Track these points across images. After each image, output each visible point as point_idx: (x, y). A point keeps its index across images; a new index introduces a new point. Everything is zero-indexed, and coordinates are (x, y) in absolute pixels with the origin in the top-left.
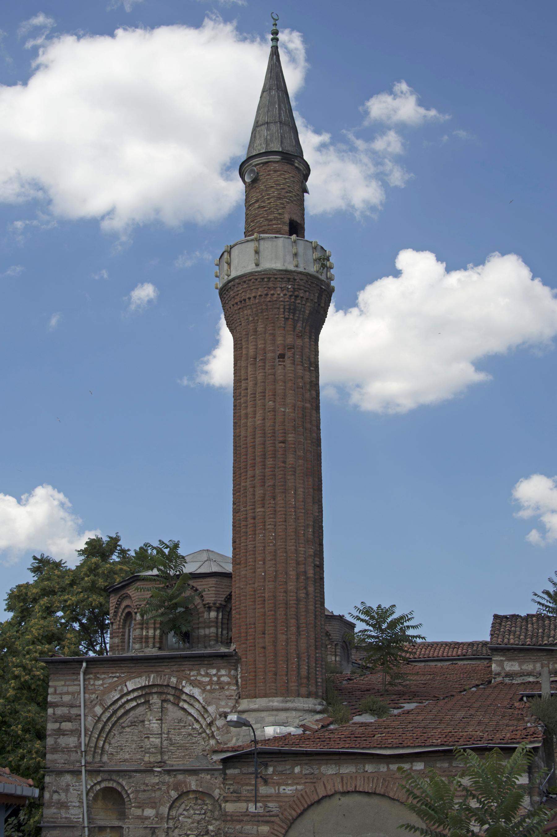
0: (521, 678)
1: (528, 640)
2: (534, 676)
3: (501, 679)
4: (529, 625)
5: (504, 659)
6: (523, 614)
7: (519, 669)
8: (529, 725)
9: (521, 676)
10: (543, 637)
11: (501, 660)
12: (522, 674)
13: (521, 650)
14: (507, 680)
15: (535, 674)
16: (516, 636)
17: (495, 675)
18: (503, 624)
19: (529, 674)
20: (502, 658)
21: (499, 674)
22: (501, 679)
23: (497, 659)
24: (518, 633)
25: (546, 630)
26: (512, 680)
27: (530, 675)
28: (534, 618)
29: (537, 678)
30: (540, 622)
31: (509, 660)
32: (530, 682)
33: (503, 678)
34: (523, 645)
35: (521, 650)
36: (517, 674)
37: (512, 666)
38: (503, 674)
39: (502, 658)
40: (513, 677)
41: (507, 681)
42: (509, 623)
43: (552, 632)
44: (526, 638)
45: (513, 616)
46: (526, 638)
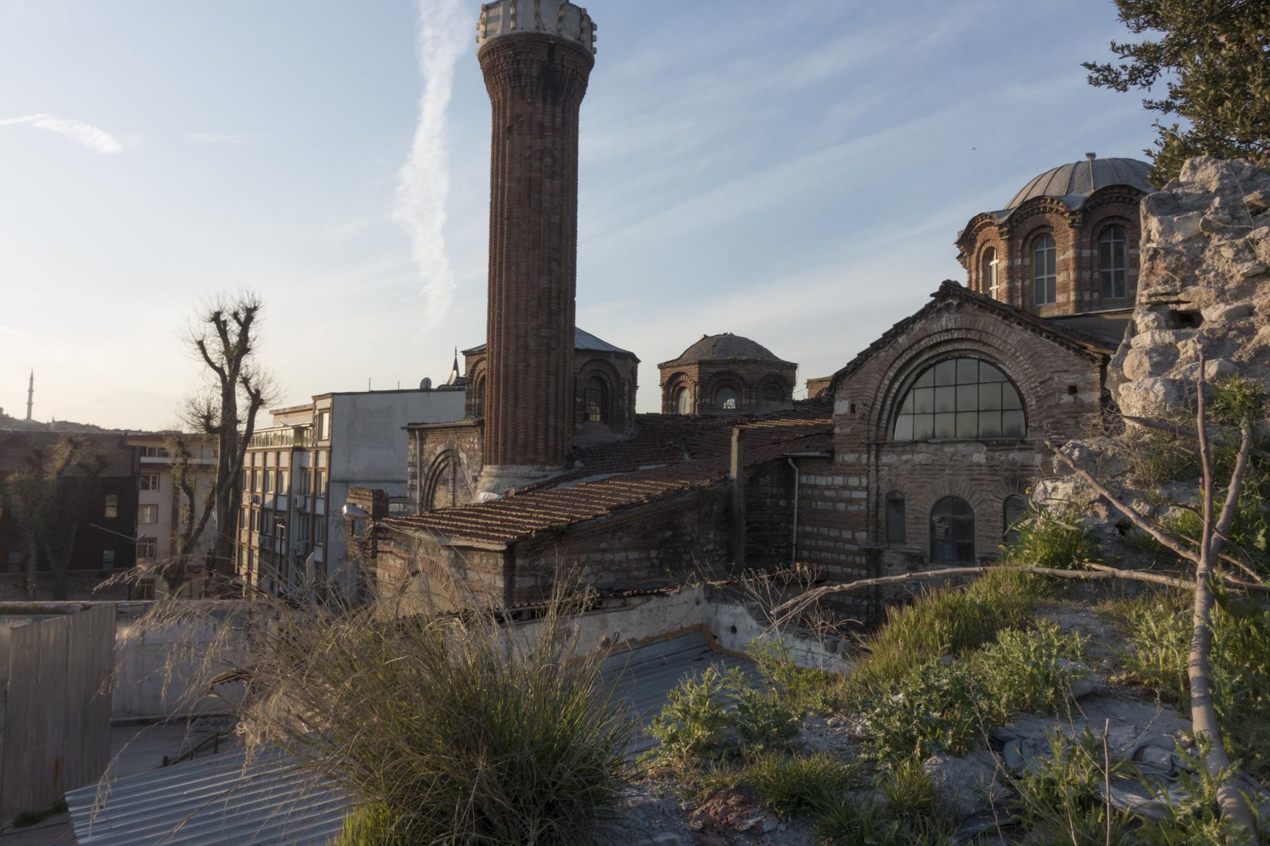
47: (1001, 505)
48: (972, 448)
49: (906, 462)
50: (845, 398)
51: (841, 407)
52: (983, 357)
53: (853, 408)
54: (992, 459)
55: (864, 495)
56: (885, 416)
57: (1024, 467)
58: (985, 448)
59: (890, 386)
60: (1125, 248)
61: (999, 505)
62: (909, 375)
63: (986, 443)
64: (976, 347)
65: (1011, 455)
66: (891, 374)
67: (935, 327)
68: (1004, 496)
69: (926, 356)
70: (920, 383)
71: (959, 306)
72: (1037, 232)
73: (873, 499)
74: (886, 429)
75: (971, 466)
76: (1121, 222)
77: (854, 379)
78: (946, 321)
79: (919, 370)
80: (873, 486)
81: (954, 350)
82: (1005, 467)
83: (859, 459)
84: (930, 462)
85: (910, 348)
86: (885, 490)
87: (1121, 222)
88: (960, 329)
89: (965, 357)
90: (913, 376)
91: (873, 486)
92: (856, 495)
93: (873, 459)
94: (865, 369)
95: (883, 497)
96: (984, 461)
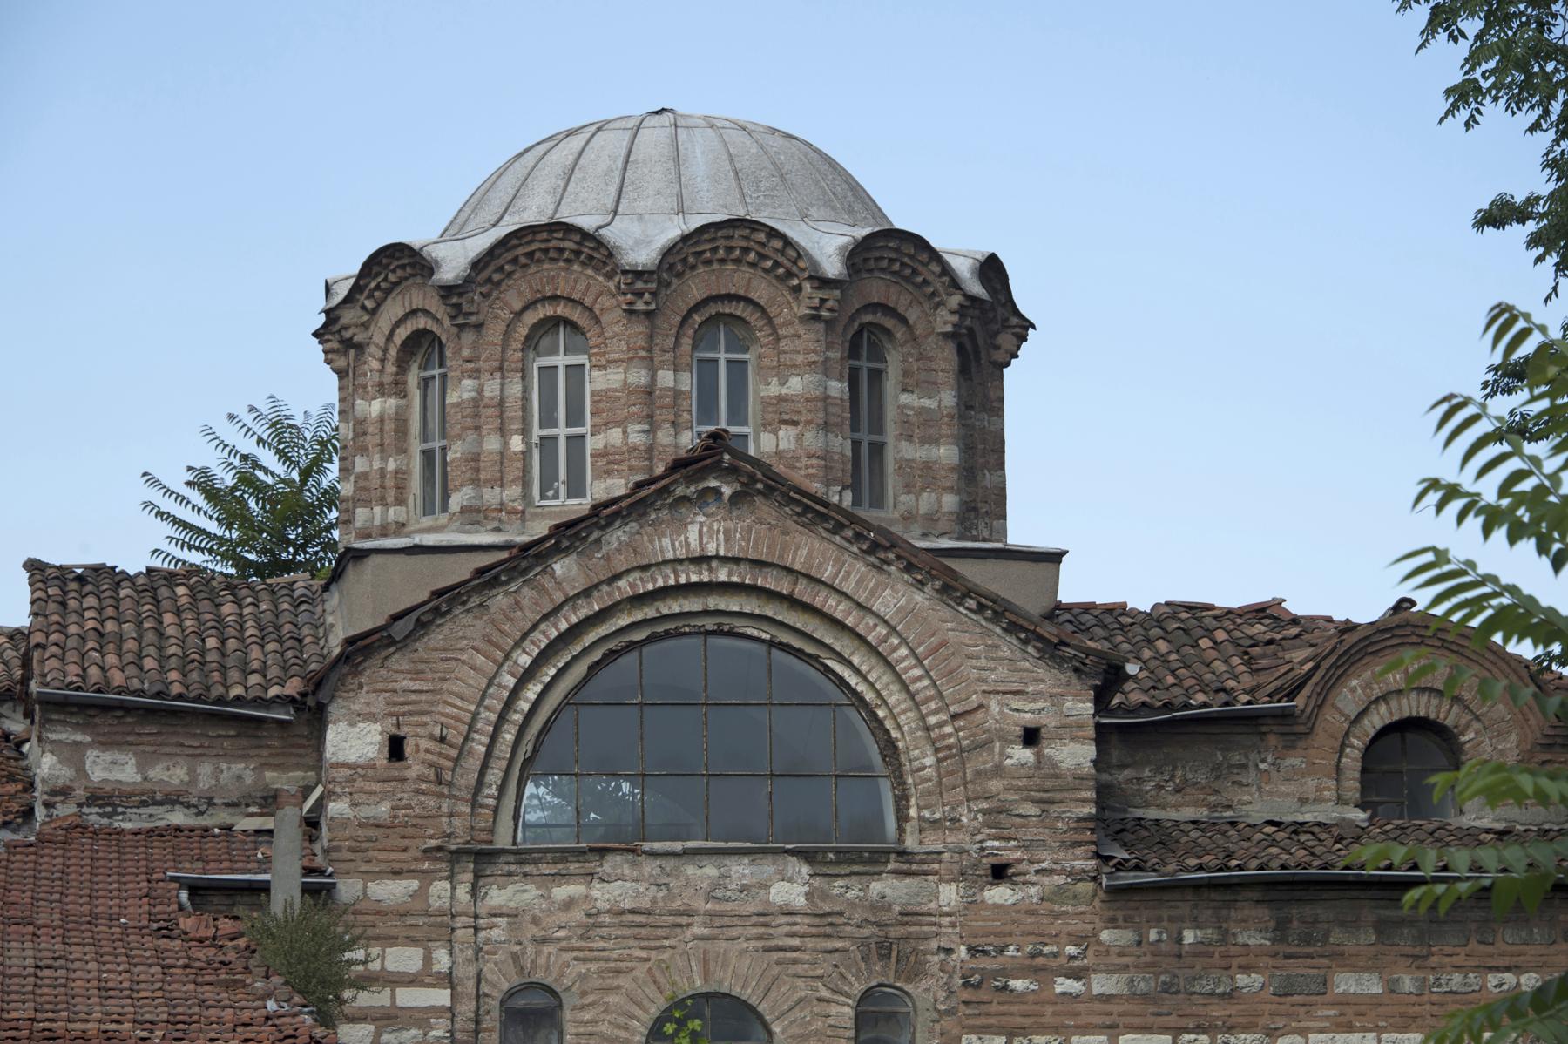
0: (145, 811)
1: (173, 675)
2: (188, 806)
3: (73, 809)
4: (168, 618)
5: (88, 739)
6: (134, 562)
7: (139, 778)
8: (271, 1005)
9: (144, 804)
10: (223, 669)
11: (77, 743)
12: (148, 798)
13: (149, 712)
14: (93, 816)
15: (194, 801)
16: (129, 657)
17: (53, 793)
18: (72, 604)
19: (173, 799)
20: (79, 737)
21: (65, 792)
22: (73, 809)
23: (63, 736)
24: (130, 645)
25: (232, 644)
26: (109, 815)
27: (174, 803)
28: (181, 590)
29: (200, 813)
30: (205, 606)
31: (105, 745)
32: (178, 829)
33: (80, 805)
34: (158, 695)
35: (149, 712)
36: (132, 794)
37: (114, 768)
38: (80, 793)
39: (79, 737)
40: (114, 806)
41: (93, 818)
42: (91, 601)
43: (255, 652)
44: (163, 670)
45: (99, 570)
46: (163, 670)
47: (849, 1012)
48: (768, 868)
49: (569, 904)
50: (370, 717)
51: (352, 740)
52: (785, 638)
53: (396, 748)
54: (825, 896)
55: (442, 997)
56: (494, 776)
57: (909, 915)
58: (805, 869)
59: (515, 693)
60: (891, 383)
61: (844, 1012)
62: (568, 665)
63: (807, 856)
64: (769, 612)
65: (876, 887)
66: (525, 660)
67: (667, 547)
68: (858, 988)
69: (624, 621)
70: (591, 693)
71: (736, 498)
72: (712, 310)
73: (467, 1008)
74: (496, 811)
75: (766, 915)
76: (889, 323)
77: (400, 661)
78: (701, 533)
79: (597, 655)
80: (466, 972)
81: (706, 613)
82: (858, 916)
83: (420, 894)
84: (645, 903)
85: (586, 593)
86: (500, 980)
87: (889, 323)
88: (736, 560)
89: (732, 634)
90: (580, 669)
91: (466, 972)
92: (409, 997)
93: (463, 893)
94: (436, 638)
95: (494, 1004)
96: (800, 902)
